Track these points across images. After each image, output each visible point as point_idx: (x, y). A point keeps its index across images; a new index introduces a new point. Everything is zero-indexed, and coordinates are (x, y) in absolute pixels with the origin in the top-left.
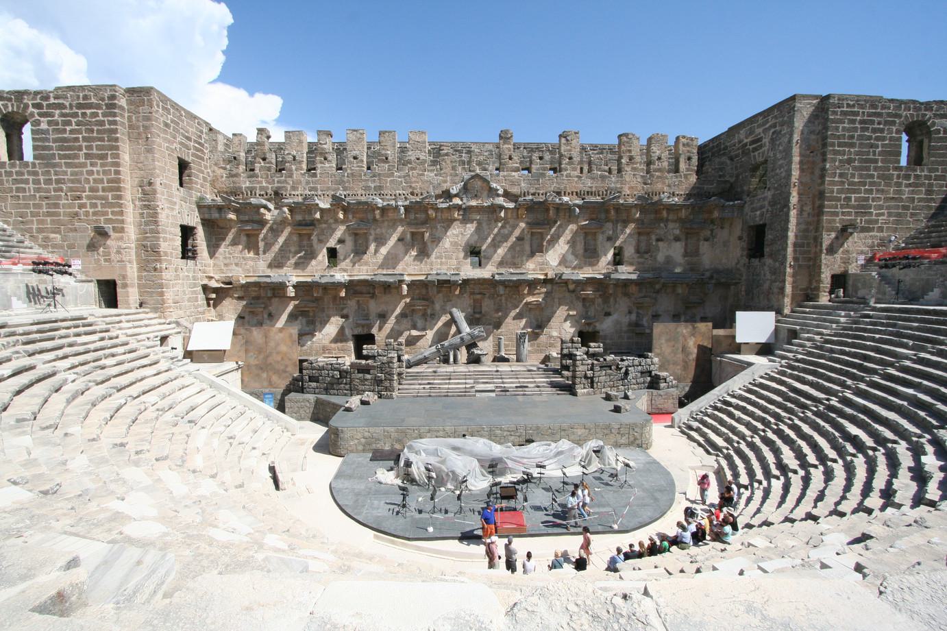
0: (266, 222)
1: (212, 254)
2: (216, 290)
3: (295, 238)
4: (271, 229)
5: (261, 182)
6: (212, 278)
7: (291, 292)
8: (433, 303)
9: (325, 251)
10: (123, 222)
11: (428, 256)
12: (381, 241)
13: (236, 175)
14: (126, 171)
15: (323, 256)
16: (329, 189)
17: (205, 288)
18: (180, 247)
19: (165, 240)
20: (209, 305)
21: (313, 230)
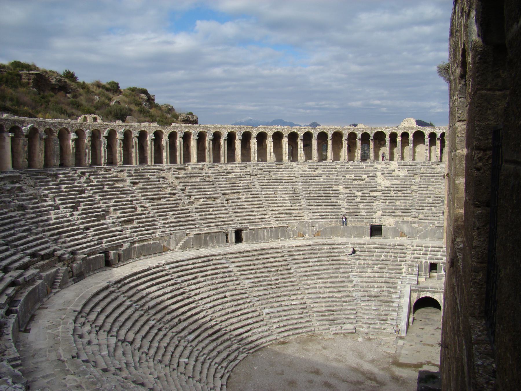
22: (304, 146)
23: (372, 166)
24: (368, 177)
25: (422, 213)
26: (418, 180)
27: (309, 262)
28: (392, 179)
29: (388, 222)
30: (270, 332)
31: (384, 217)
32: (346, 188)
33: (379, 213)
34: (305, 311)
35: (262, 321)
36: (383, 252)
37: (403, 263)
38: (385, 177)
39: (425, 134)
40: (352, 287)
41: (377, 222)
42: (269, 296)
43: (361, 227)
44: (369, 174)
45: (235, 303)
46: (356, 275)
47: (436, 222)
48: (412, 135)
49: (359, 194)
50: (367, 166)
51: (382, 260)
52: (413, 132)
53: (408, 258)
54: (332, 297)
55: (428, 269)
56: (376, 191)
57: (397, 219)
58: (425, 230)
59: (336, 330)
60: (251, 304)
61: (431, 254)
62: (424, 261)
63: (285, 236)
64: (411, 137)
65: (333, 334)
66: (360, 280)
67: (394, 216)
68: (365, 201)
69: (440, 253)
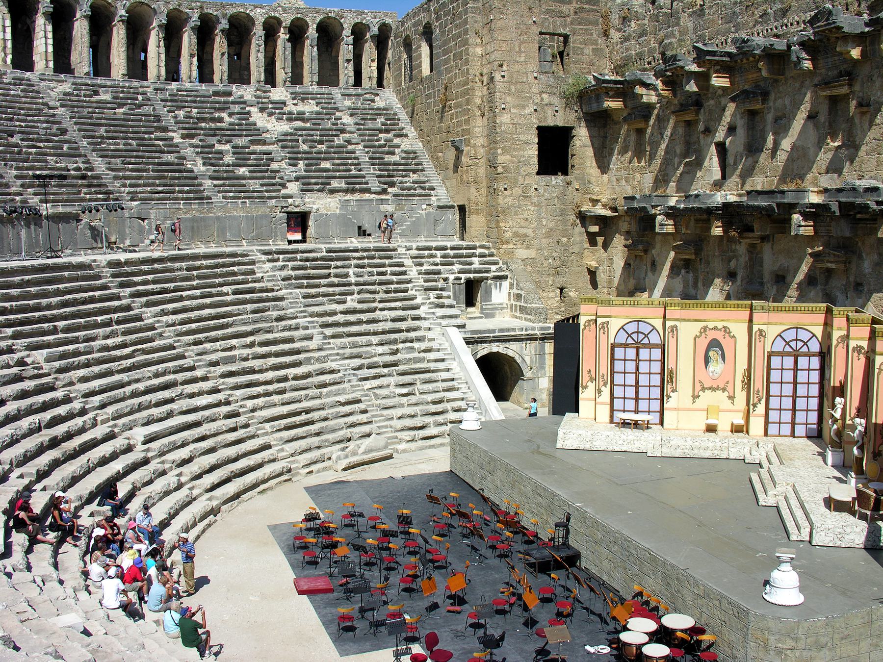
0: (650, 107)
1: (603, 166)
2: (601, 220)
3: (681, 131)
4: (658, 115)
5: (649, 42)
6: (598, 201)
7: (665, 226)
8: (860, 257)
9: (713, 148)
10: (468, 132)
11: (857, 148)
12: (782, 126)
13: (626, 39)
14: (475, 68)
15: (712, 162)
16: (718, 33)
17: (583, 218)
18: (535, 161)
19: (505, 151)
20: (593, 242)
21: (697, 113)
22: (54, 32)
23: (230, 94)
24: (231, 115)
25: (392, 185)
26: (347, 119)
27: (181, 299)
28: (290, 120)
29: (321, 205)
30: (184, 491)
31: (309, 194)
32: (191, 136)
33: (293, 188)
34: (242, 420)
35: (146, 462)
36: (349, 267)
37: (409, 286)
38: (271, 114)
39: (345, 26)
40: (320, 350)
41: (297, 204)
42: (128, 390)
43: (261, 217)
44: (229, 108)
45: (47, 416)
46: (313, 322)
47: (433, 198)
48: (315, 26)
49: (227, 147)
50: (216, 94)
51: (357, 284)
52: (318, 20)
53: (413, 272)
54: (285, 379)
55: (463, 297)
56: (264, 142)
57: (339, 196)
58: (412, 217)
59: (346, 457)
60: (91, 415)
61: (461, 263)
62: (452, 277)
63: (76, 244)
64: (312, 32)
65: (345, 469)
66: (329, 332)
67: (333, 191)
68: (250, 162)
69: (476, 260)
